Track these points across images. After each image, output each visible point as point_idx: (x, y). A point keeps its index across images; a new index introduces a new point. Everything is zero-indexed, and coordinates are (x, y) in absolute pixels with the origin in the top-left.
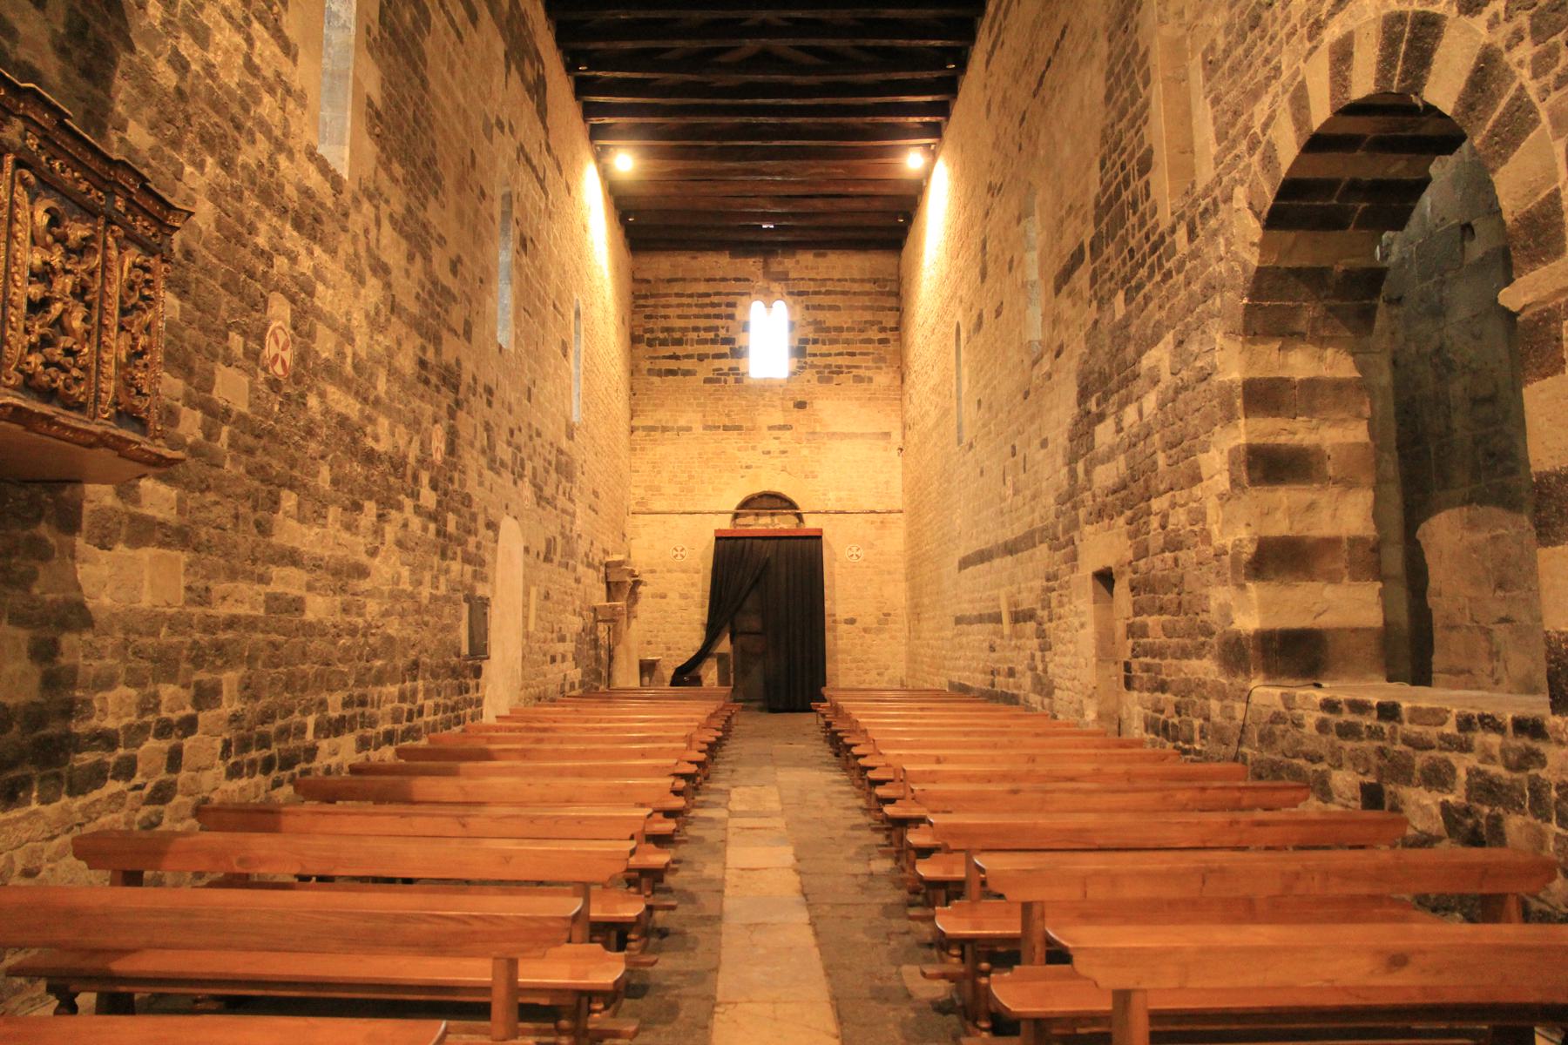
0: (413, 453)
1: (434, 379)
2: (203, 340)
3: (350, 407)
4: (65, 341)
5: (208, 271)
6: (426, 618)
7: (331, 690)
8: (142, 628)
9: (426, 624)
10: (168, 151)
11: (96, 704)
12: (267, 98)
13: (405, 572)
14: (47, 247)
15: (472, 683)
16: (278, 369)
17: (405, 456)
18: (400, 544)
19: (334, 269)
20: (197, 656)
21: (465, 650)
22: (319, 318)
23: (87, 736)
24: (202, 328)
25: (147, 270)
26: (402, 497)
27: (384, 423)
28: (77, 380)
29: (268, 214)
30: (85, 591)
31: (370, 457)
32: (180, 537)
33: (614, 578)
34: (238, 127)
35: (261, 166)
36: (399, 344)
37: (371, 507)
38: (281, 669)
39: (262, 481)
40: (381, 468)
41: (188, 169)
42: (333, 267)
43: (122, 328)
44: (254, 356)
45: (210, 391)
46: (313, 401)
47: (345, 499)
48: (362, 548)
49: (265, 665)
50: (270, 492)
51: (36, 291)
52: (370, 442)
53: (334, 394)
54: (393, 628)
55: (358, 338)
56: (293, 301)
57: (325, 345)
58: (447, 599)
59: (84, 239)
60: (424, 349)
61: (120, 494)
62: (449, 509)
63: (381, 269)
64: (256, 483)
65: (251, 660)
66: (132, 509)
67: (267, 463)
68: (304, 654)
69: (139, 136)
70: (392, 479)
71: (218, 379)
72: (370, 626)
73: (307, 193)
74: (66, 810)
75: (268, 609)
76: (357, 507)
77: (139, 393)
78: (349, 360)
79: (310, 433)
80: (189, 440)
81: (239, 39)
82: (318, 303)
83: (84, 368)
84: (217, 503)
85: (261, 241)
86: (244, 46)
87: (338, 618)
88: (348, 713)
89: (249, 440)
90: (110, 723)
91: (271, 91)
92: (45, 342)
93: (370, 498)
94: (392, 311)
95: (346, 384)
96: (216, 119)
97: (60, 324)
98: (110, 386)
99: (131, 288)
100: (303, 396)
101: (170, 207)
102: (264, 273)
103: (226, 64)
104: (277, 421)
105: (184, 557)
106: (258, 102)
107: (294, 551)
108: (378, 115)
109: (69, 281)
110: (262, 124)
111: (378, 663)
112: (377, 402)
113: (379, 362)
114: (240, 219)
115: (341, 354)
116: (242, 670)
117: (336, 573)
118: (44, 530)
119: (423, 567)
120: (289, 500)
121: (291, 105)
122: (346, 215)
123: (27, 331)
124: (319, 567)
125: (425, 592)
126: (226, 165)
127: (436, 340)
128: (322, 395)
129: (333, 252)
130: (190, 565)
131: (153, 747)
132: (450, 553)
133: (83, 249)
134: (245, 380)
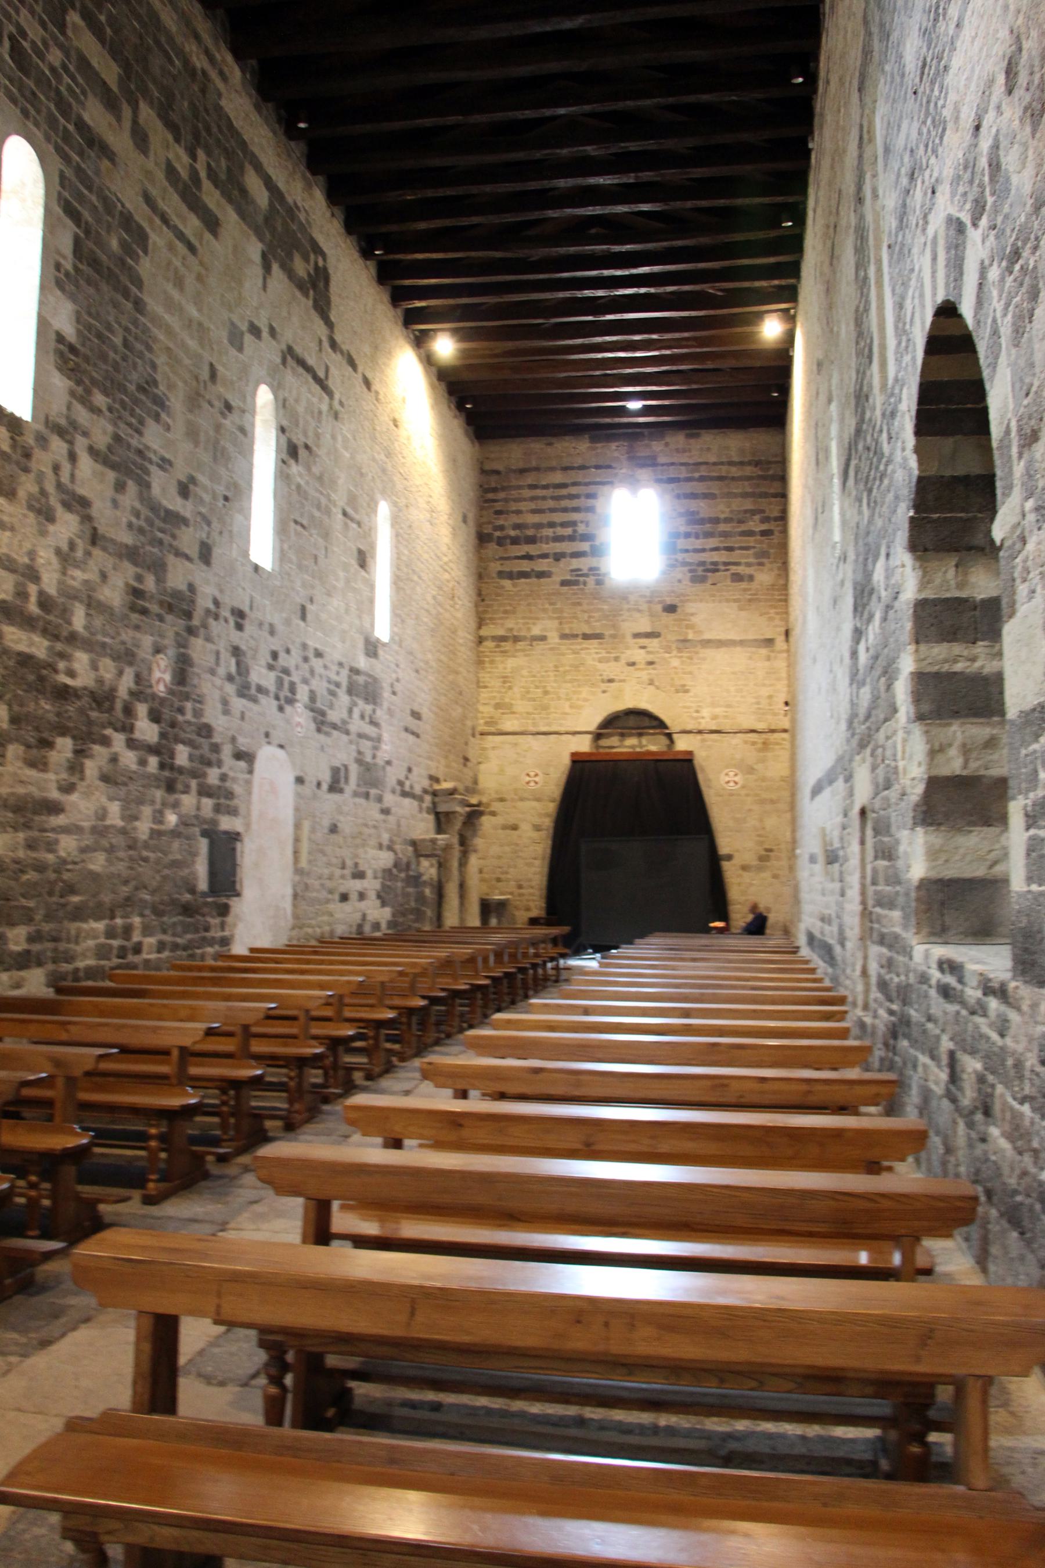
0: (126, 683)
1: (154, 608)
3: (38, 646)
6: (145, 853)
7: (12, 924)
9: (146, 860)
13: (114, 809)
15: (215, 921)
17: (113, 689)
18: (105, 778)
21: (203, 885)
26: (109, 732)
31: (63, 693)
33: (442, 808)
36: (104, 576)
48: (53, 786)
52: (64, 679)
54: (98, 863)
58: (175, 833)
60: (139, 578)
62: (178, 740)
63: (78, 504)
70: (94, 714)
72: (64, 862)
87: (21, 854)
88: (36, 947)
93: (63, 734)
94: (94, 543)
95: (28, 623)
108: (72, 349)
111: (76, 899)
112: (72, 638)
113: (75, 598)
119: (140, 802)
122: (28, 455)
125: (143, 828)
127: (159, 568)
132: (180, 786)
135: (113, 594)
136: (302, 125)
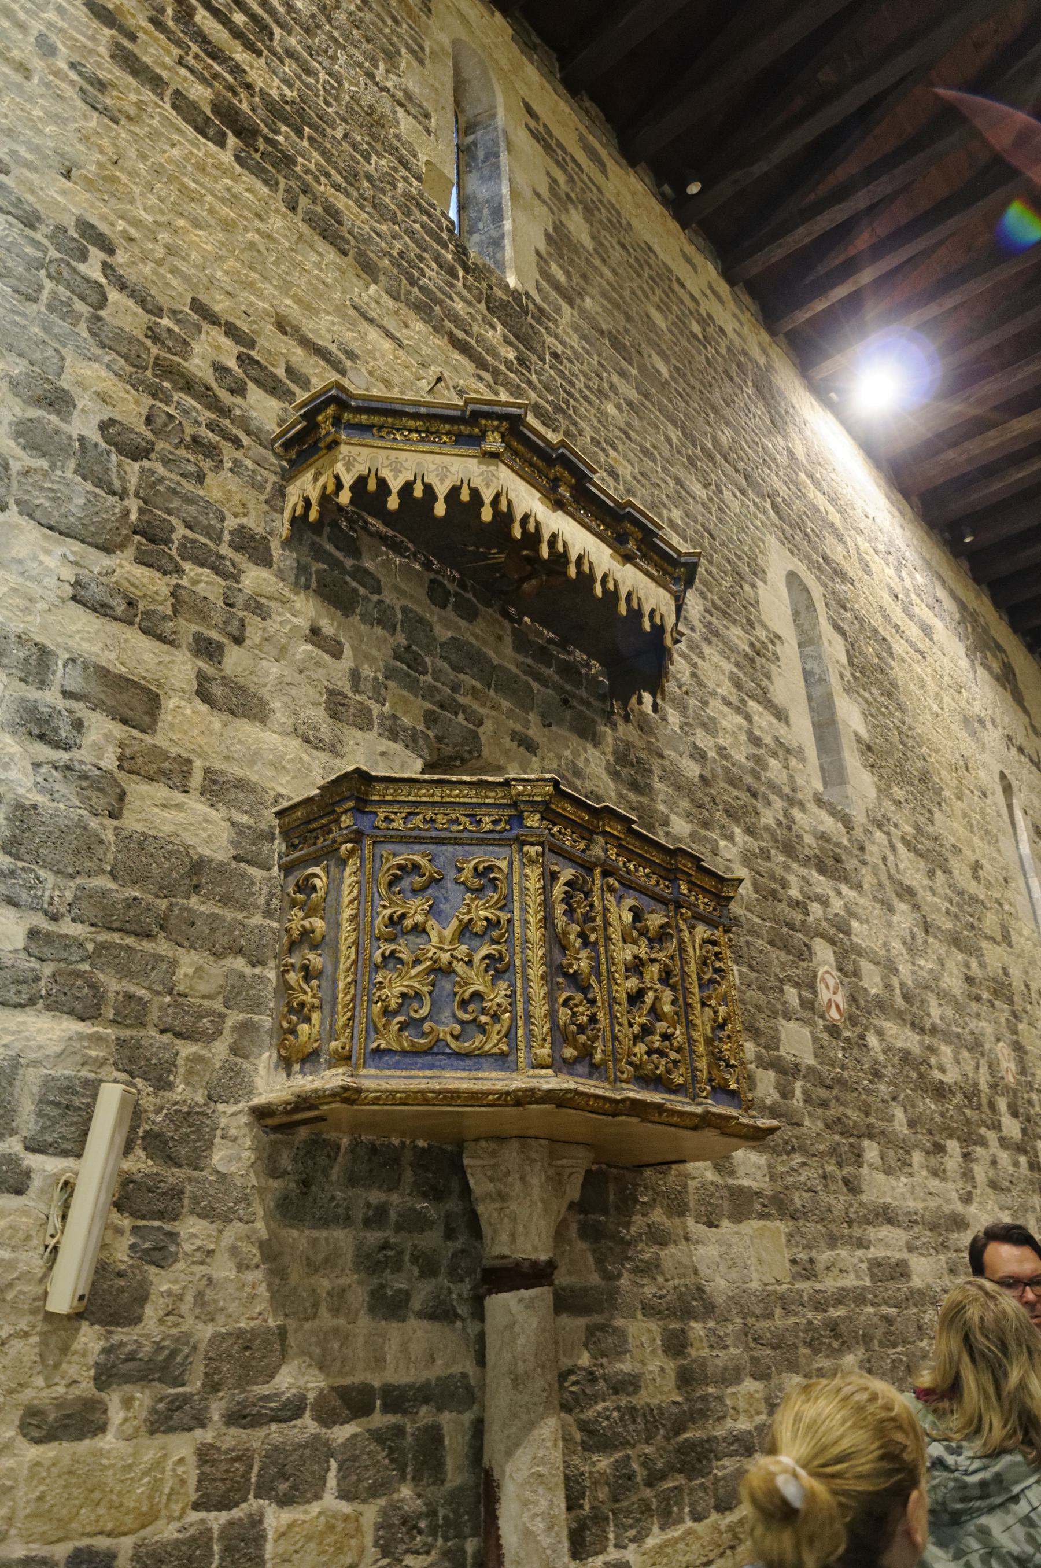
0: (983, 1080)
1: (985, 995)
2: (762, 999)
4: (662, 1026)
5: (754, 932)
8: (758, 1312)
10: (703, 832)
11: (728, 1402)
12: (773, 762)
14: (635, 942)
16: (834, 1014)
17: (976, 1084)
18: (993, 1185)
19: (864, 902)
20: (813, 1339)
22: (860, 955)
24: (759, 988)
25: (714, 943)
26: (983, 1130)
27: (946, 1051)
28: (676, 1062)
29: (795, 866)
30: (702, 1274)
31: (940, 1092)
32: (778, 1205)
34: (754, 795)
35: (780, 824)
37: (953, 1146)
38: (899, 1349)
39: (842, 1134)
40: (955, 1101)
41: (722, 843)
42: (862, 901)
43: (704, 1004)
44: (808, 1005)
45: (777, 1049)
46: (872, 1040)
47: (925, 1140)
48: (954, 1195)
49: (882, 1344)
50: (851, 1145)
51: (633, 983)
52: (937, 1074)
53: (890, 1027)
55: (900, 968)
56: (832, 942)
57: (872, 982)
59: (662, 927)
60: (967, 966)
61: (718, 1168)
63: (907, 892)
64: (837, 1137)
65: (867, 1339)
66: (730, 1182)
67: (844, 1115)
68: (920, 1327)
69: (681, 827)
70: (968, 1112)
71: (783, 1036)
73: (823, 837)
74: (715, 1528)
75: (873, 1276)
76: (939, 1149)
77: (728, 1065)
78: (898, 991)
79: (877, 1075)
80: (768, 1102)
81: (739, 719)
82: (856, 940)
83: (679, 1050)
84: (804, 1164)
85: (794, 892)
86: (745, 723)
89: (823, 1093)
90: (743, 1425)
91: (774, 755)
92: (646, 1030)
93: (950, 1137)
94: (927, 932)
95: (899, 1016)
96: (736, 793)
97: (655, 1012)
98: (702, 1064)
99: (705, 964)
100: (862, 1037)
101: (721, 880)
102: (803, 922)
103: (737, 743)
104: (843, 1067)
105: (782, 1227)
106: (765, 767)
107: (886, 1207)
108: (869, 748)
109: (655, 968)
110: (771, 785)
112: (934, 1030)
114: (772, 877)
115: (887, 986)
116: (861, 1352)
117: (933, 1227)
118: (658, 1216)
120: (871, 1151)
121: (793, 762)
122: (862, 849)
123: (631, 1025)
124: (916, 1222)
126: (749, 831)
127: (976, 952)
128: (880, 1033)
129: (859, 887)
130: (790, 1235)
133: (661, 937)
134: (806, 1031)
135: (953, 983)
136: (968, 540)
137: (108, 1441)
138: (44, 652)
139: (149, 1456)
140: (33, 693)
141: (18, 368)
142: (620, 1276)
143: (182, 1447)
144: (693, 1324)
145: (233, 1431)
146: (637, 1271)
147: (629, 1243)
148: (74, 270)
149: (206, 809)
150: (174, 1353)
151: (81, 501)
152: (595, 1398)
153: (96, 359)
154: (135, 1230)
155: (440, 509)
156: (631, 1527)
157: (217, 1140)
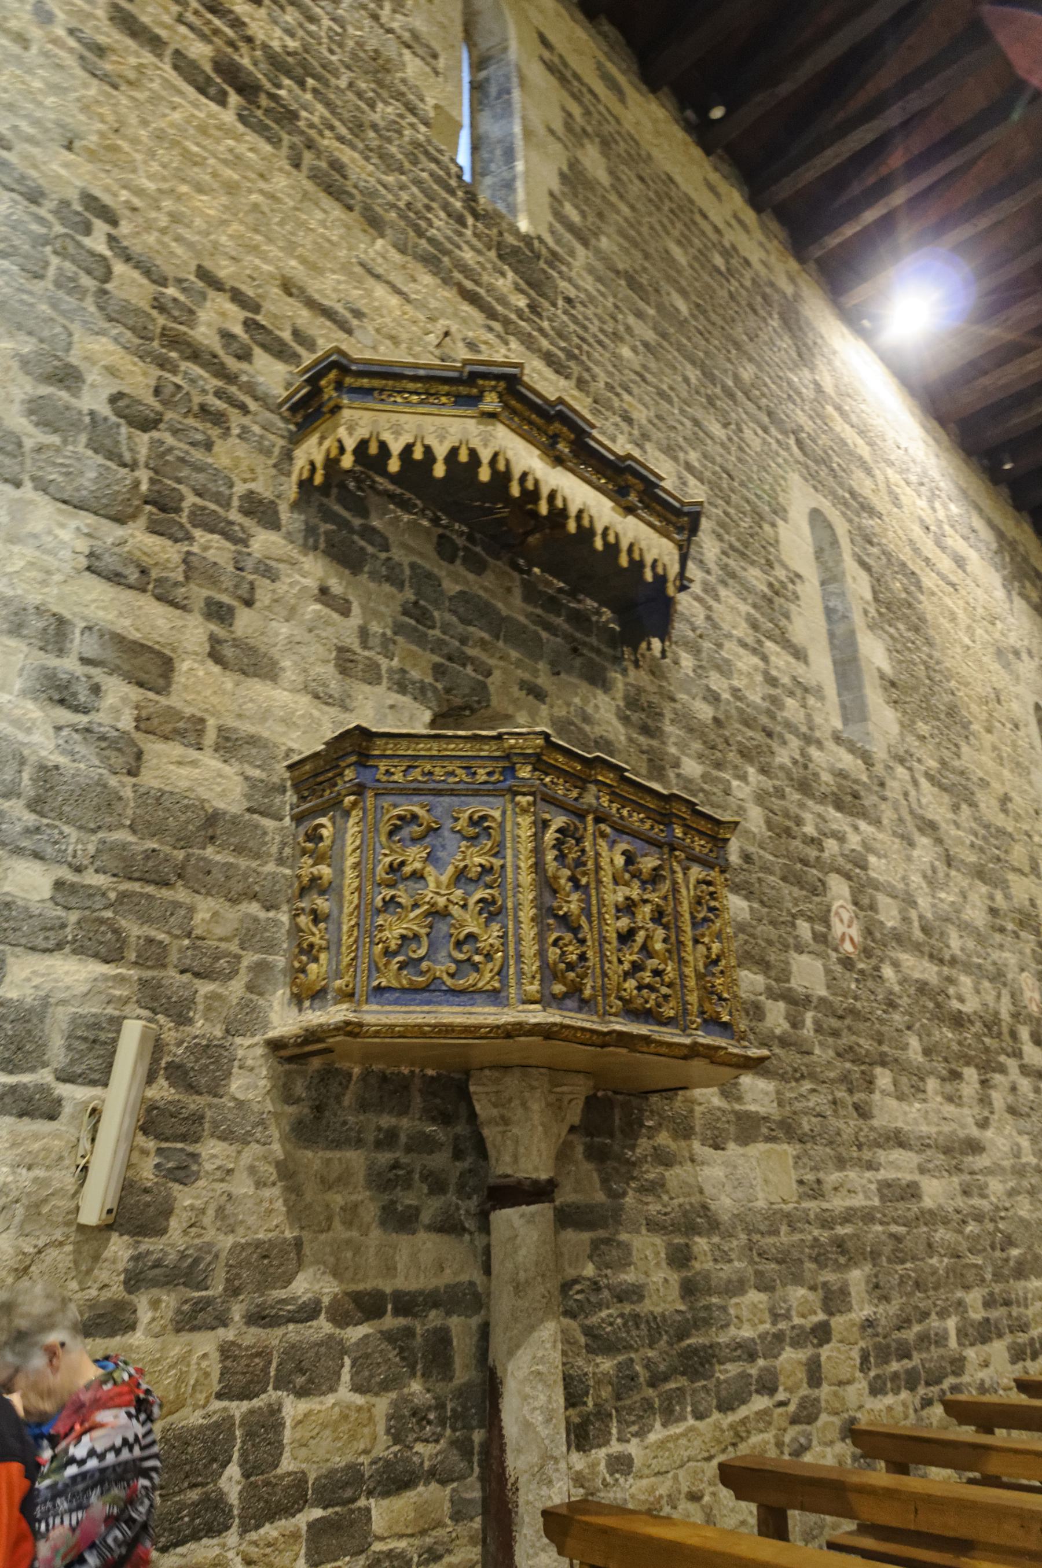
1: (1010, 926)
2: (772, 933)
3: (928, 972)
4: (652, 963)
5: (767, 869)
7: (967, 1288)
8: (763, 1228)
10: (715, 773)
11: (732, 1311)
12: (790, 702)
13: (1025, 1142)
14: (627, 884)
16: (848, 947)
17: (996, 1014)
18: (1012, 1111)
19: (883, 838)
20: (819, 1255)
22: (877, 889)
23: (728, 1346)
24: (771, 923)
25: (709, 883)
26: (1002, 1058)
27: (966, 982)
28: (666, 997)
29: (810, 803)
30: (707, 1193)
31: (958, 1021)
32: (787, 1129)
34: (770, 735)
35: (795, 762)
36: (964, 895)
37: (971, 1074)
38: (908, 1265)
39: (853, 1062)
40: (973, 1030)
41: (735, 783)
42: (880, 836)
43: (696, 941)
44: (822, 939)
45: (788, 981)
46: (888, 972)
47: (941, 1068)
48: (970, 1121)
49: (889, 1261)
50: (863, 1072)
51: (624, 923)
52: (955, 1004)
53: (907, 959)
55: (920, 901)
56: (848, 877)
57: (889, 915)
59: (655, 869)
60: (992, 898)
61: (725, 1094)
63: (929, 827)
64: (848, 1065)
65: (874, 1256)
66: (737, 1107)
67: (856, 1043)
68: (930, 1245)
69: (691, 768)
70: (987, 1040)
71: (794, 968)
72: (997, 1209)
73: (841, 774)
74: (717, 1426)
75: (883, 1198)
76: (956, 1075)
77: (721, 999)
78: (916, 924)
79: (892, 1005)
80: (778, 1031)
81: (755, 660)
82: (873, 874)
83: (670, 985)
84: (814, 1090)
85: (809, 829)
86: (761, 664)
87: (960, 1202)
88: (995, 1314)
89: (834, 1023)
90: (747, 1333)
91: (791, 694)
92: (637, 967)
93: (967, 1064)
94: (949, 865)
95: (917, 948)
96: (750, 733)
97: (646, 950)
98: (693, 998)
99: (699, 903)
100: (877, 969)
101: (718, 823)
102: (818, 858)
103: (752, 685)
104: (856, 998)
105: (790, 1150)
106: (781, 707)
107: (898, 1132)
108: (893, 684)
109: (647, 909)
110: (788, 725)
111: (1015, 1252)
112: (953, 961)
113: (947, 920)
114: (787, 815)
115: (906, 919)
116: (868, 1268)
117: (947, 1151)
118: (663, 1138)
120: (884, 1078)
121: (811, 701)
122: (882, 785)
123: (620, 962)
124: (929, 1146)
126: (764, 771)
127: (1003, 884)
128: (896, 965)
129: (877, 822)
130: (798, 1157)
131: (790, 1357)
133: (655, 878)
134: (819, 964)
135: (976, 914)
136: (1007, 467)
137: (138, 1338)
138: (61, 622)
139: (175, 1352)
140: (52, 661)
141: (27, 346)
142: (624, 1194)
143: (206, 1344)
144: (697, 1239)
145: (253, 1330)
146: (642, 1190)
147: (634, 1164)
148: (79, 245)
149: (219, 765)
150: (197, 1261)
151: (92, 475)
152: (600, 1305)
153: (102, 333)
154: (160, 1151)
155: (439, 470)
156: (633, 1423)
157: (235, 1070)
